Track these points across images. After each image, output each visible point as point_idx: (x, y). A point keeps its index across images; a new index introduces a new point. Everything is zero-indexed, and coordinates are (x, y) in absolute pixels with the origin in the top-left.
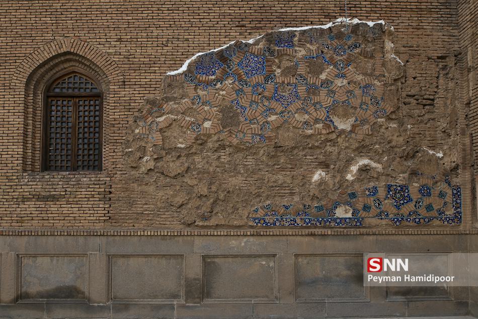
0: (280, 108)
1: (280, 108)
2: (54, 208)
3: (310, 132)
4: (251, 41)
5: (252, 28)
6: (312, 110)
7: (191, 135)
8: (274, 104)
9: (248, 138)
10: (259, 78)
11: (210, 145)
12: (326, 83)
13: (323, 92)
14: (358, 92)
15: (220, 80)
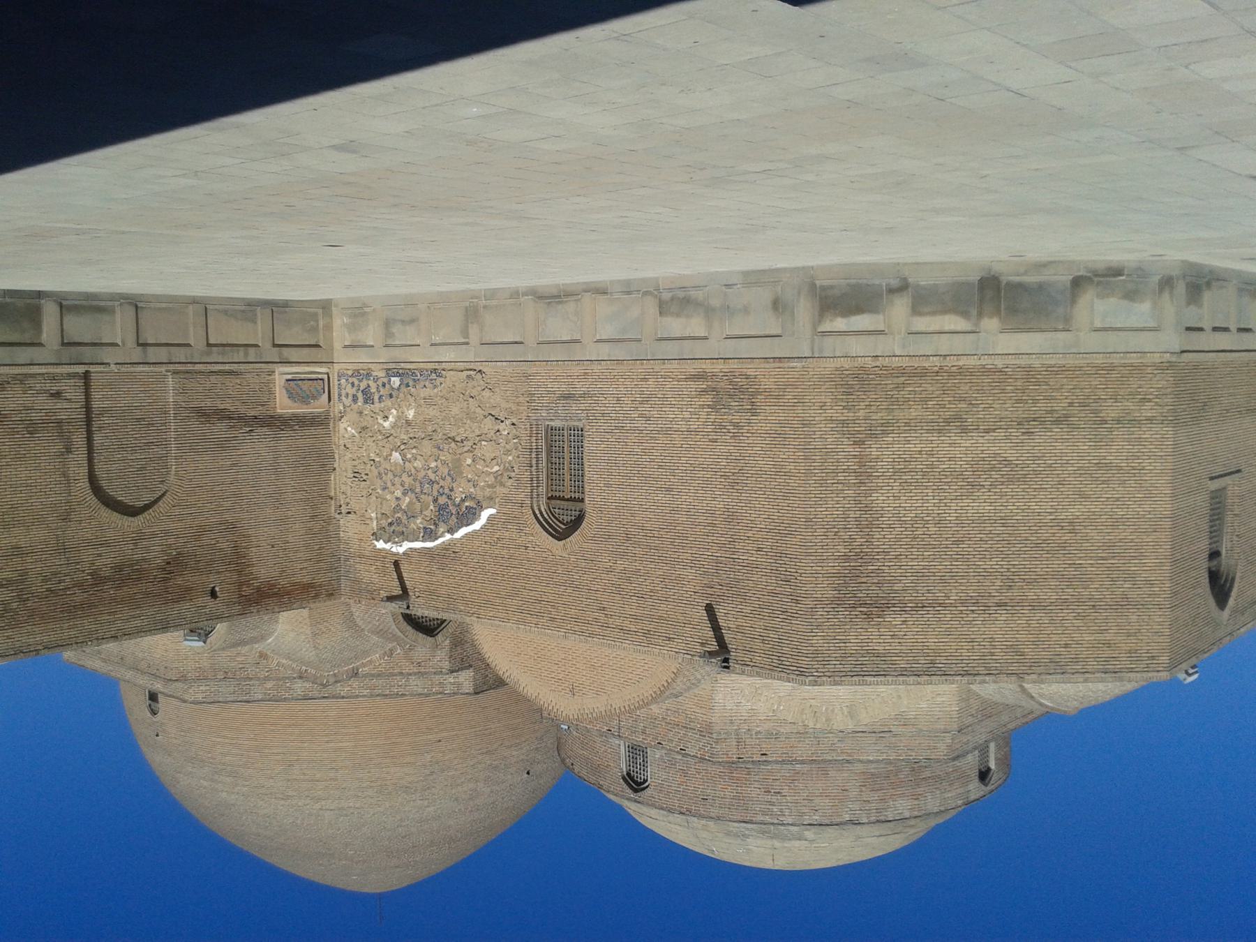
0: (430, 472)
1: (430, 472)
2: (564, 389)
3: (414, 451)
4: (448, 536)
5: (447, 550)
6: (413, 471)
7: (478, 453)
8: (432, 476)
9: (446, 447)
10: (442, 500)
11: (470, 443)
12: (405, 494)
13: (407, 486)
14: (389, 484)
15: (463, 501)
